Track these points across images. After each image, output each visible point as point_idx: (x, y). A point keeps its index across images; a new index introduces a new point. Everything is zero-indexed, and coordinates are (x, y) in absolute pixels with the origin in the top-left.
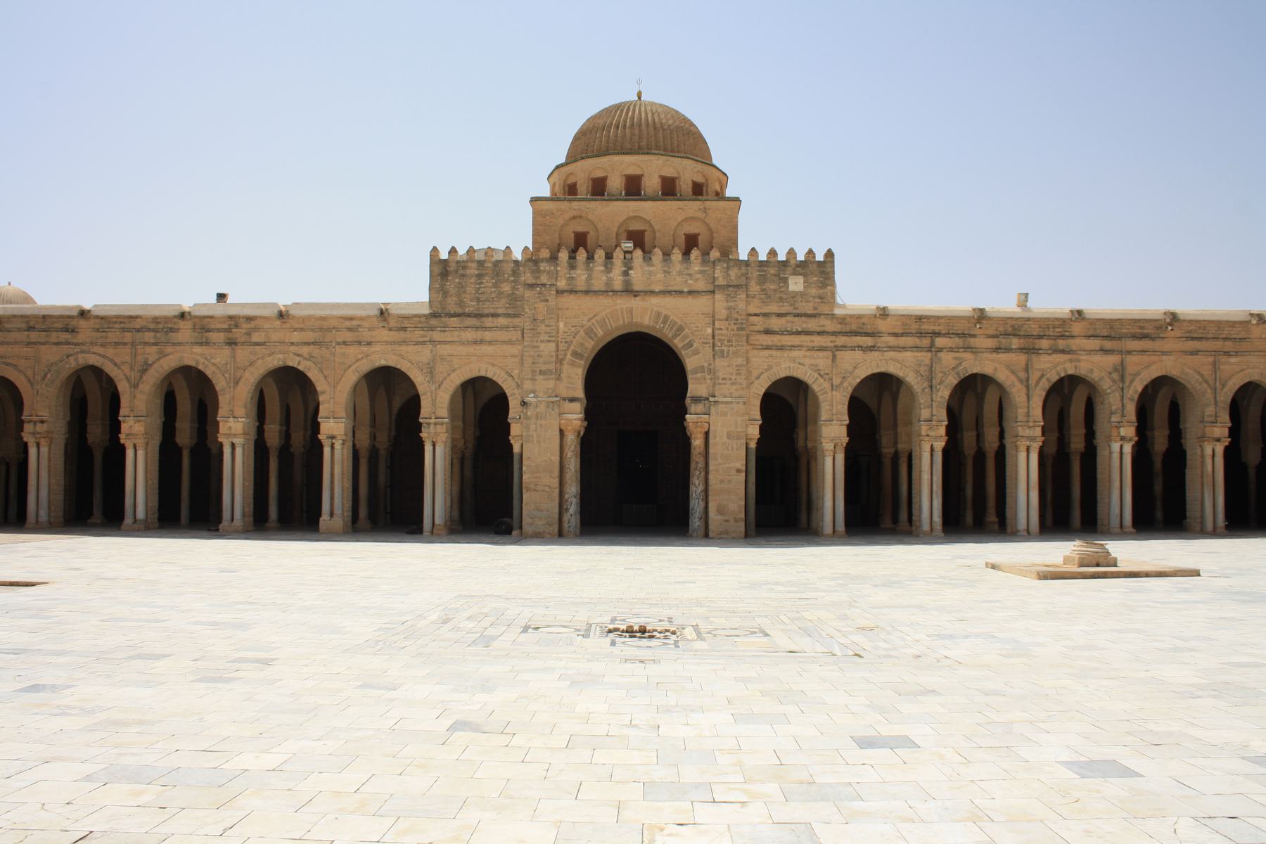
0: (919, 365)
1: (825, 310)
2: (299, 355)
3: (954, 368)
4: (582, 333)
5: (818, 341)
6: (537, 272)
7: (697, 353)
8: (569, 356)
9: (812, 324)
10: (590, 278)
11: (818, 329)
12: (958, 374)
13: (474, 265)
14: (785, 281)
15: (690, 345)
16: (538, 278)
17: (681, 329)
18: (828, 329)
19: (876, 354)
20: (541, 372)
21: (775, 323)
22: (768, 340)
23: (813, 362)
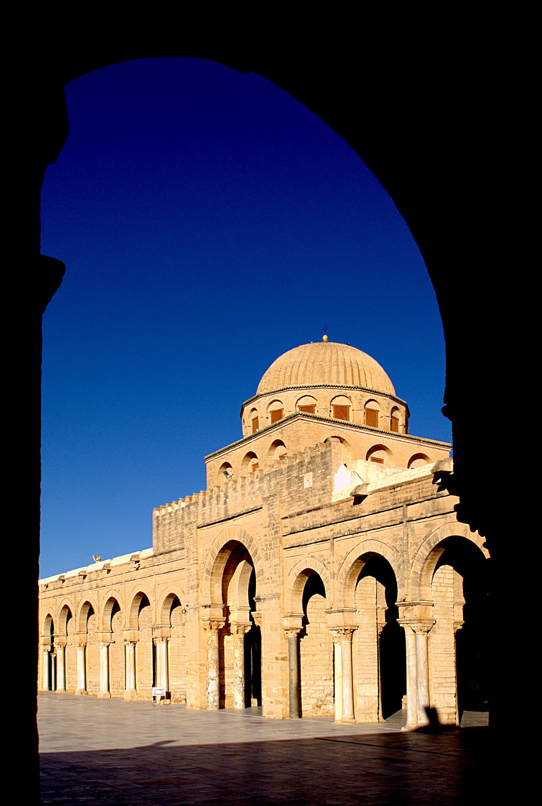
0: (395, 540)
1: (326, 501)
2: (115, 590)
3: (426, 537)
4: (210, 554)
5: (325, 532)
6: (189, 513)
7: (259, 559)
8: (205, 574)
9: (317, 517)
10: (211, 512)
11: (322, 521)
12: (429, 543)
13: (168, 516)
14: (301, 480)
15: (256, 552)
16: (189, 518)
17: (251, 540)
18: (329, 520)
19: (362, 537)
20: (192, 588)
21: (298, 522)
22: (293, 539)
23: (321, 553)
